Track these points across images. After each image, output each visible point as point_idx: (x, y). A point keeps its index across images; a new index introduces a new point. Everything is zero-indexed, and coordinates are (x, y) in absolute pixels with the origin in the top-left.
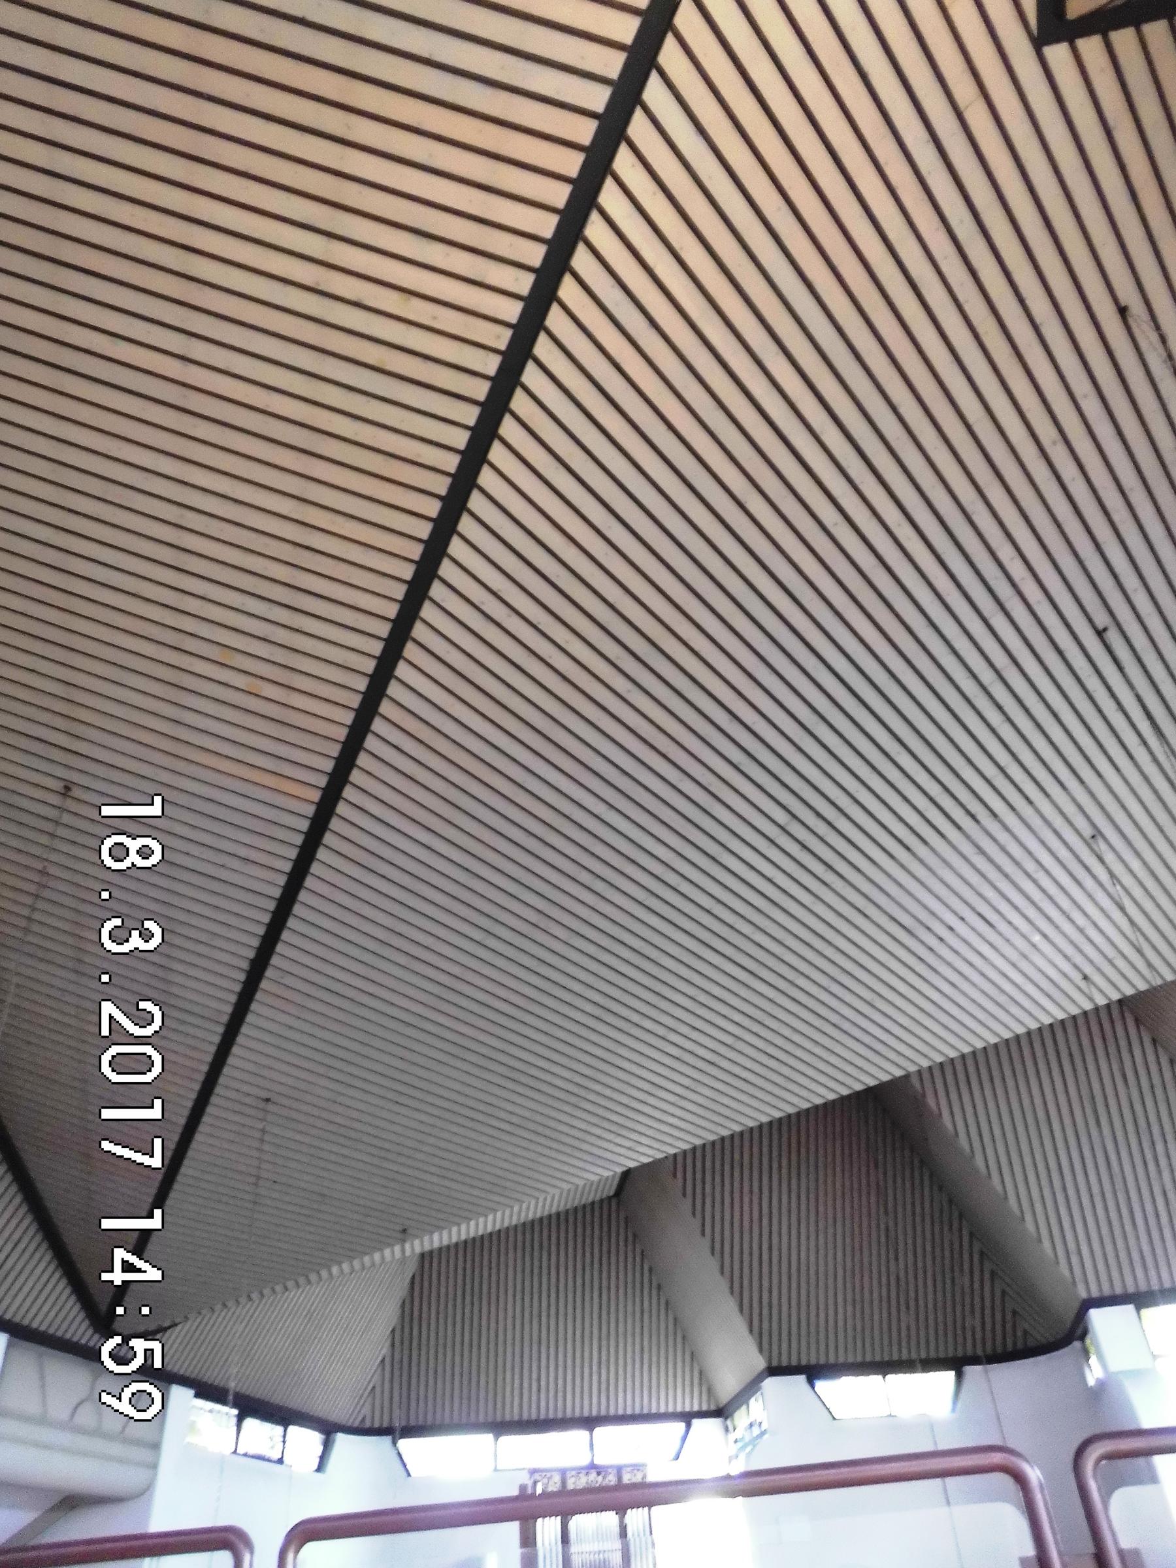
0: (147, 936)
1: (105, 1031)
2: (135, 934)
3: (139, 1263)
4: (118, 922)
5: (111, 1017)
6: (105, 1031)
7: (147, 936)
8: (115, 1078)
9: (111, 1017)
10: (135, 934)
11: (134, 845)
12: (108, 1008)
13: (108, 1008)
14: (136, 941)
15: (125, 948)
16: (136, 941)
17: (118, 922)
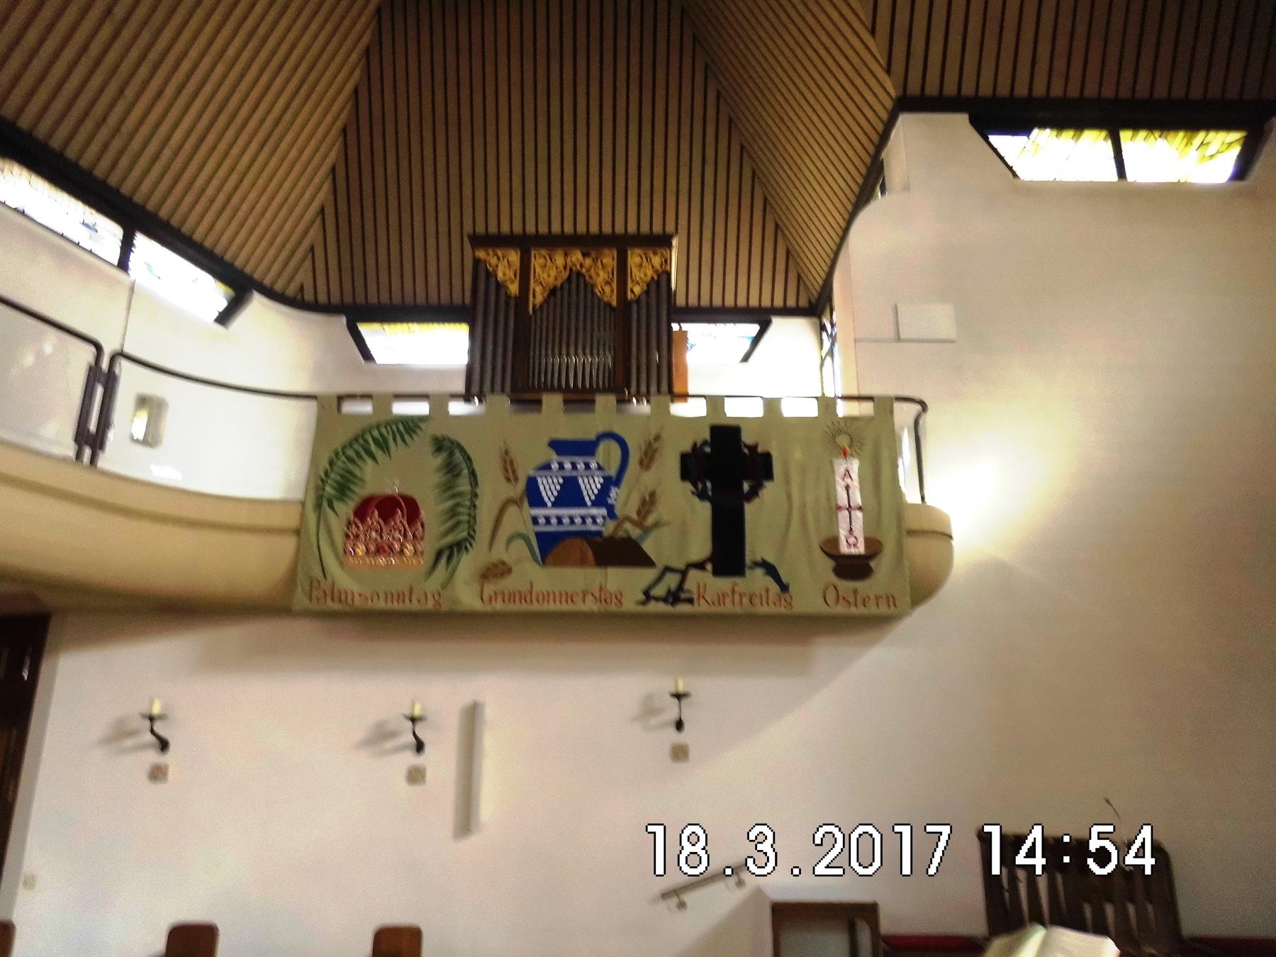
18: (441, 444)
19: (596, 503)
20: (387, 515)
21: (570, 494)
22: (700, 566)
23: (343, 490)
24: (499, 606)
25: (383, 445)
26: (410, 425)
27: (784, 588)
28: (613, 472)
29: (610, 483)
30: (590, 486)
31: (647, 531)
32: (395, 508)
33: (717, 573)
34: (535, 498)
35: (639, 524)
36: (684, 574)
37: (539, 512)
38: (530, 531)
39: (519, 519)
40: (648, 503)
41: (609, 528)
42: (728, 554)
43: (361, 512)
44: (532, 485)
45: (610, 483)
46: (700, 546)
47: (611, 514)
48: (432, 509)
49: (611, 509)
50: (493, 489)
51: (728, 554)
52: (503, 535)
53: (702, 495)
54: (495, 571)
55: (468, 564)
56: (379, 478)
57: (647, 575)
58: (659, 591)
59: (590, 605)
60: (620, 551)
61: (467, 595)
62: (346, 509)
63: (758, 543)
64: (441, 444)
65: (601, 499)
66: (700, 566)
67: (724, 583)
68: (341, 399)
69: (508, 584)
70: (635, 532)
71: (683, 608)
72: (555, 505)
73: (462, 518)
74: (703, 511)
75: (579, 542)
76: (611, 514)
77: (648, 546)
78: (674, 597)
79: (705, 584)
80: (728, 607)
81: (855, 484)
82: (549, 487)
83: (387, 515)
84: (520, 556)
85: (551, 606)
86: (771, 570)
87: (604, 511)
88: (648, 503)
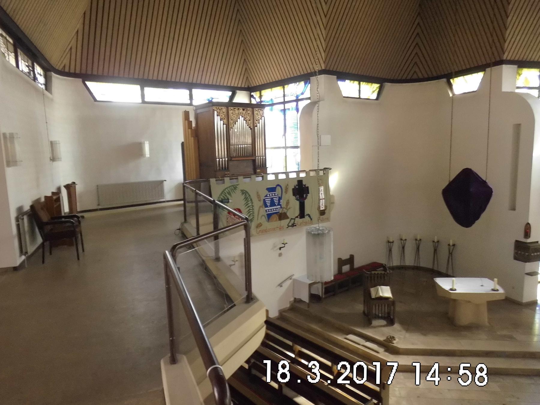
2: (313, 371)
3: (432, 371)
11: (281, 371)
27: (311, 219)
31: (288, 210)
35: (286, 209)
37: (267, 209)
38: (265, 214)
39: (263, 211)
40: (288, 203)
46: (297, 213)
49: (281, 205)
52: (260, 216)
53: (297, 199)
60: (282, 216)
63: (307, 211)
72: (271, 206)
74: (298, 203)
79: (298, 220)
81: (323, 195)
82: (268, 204)
84: (263, 220)
86: (309, 215)
87: (279, 207)
88: (288, 203)
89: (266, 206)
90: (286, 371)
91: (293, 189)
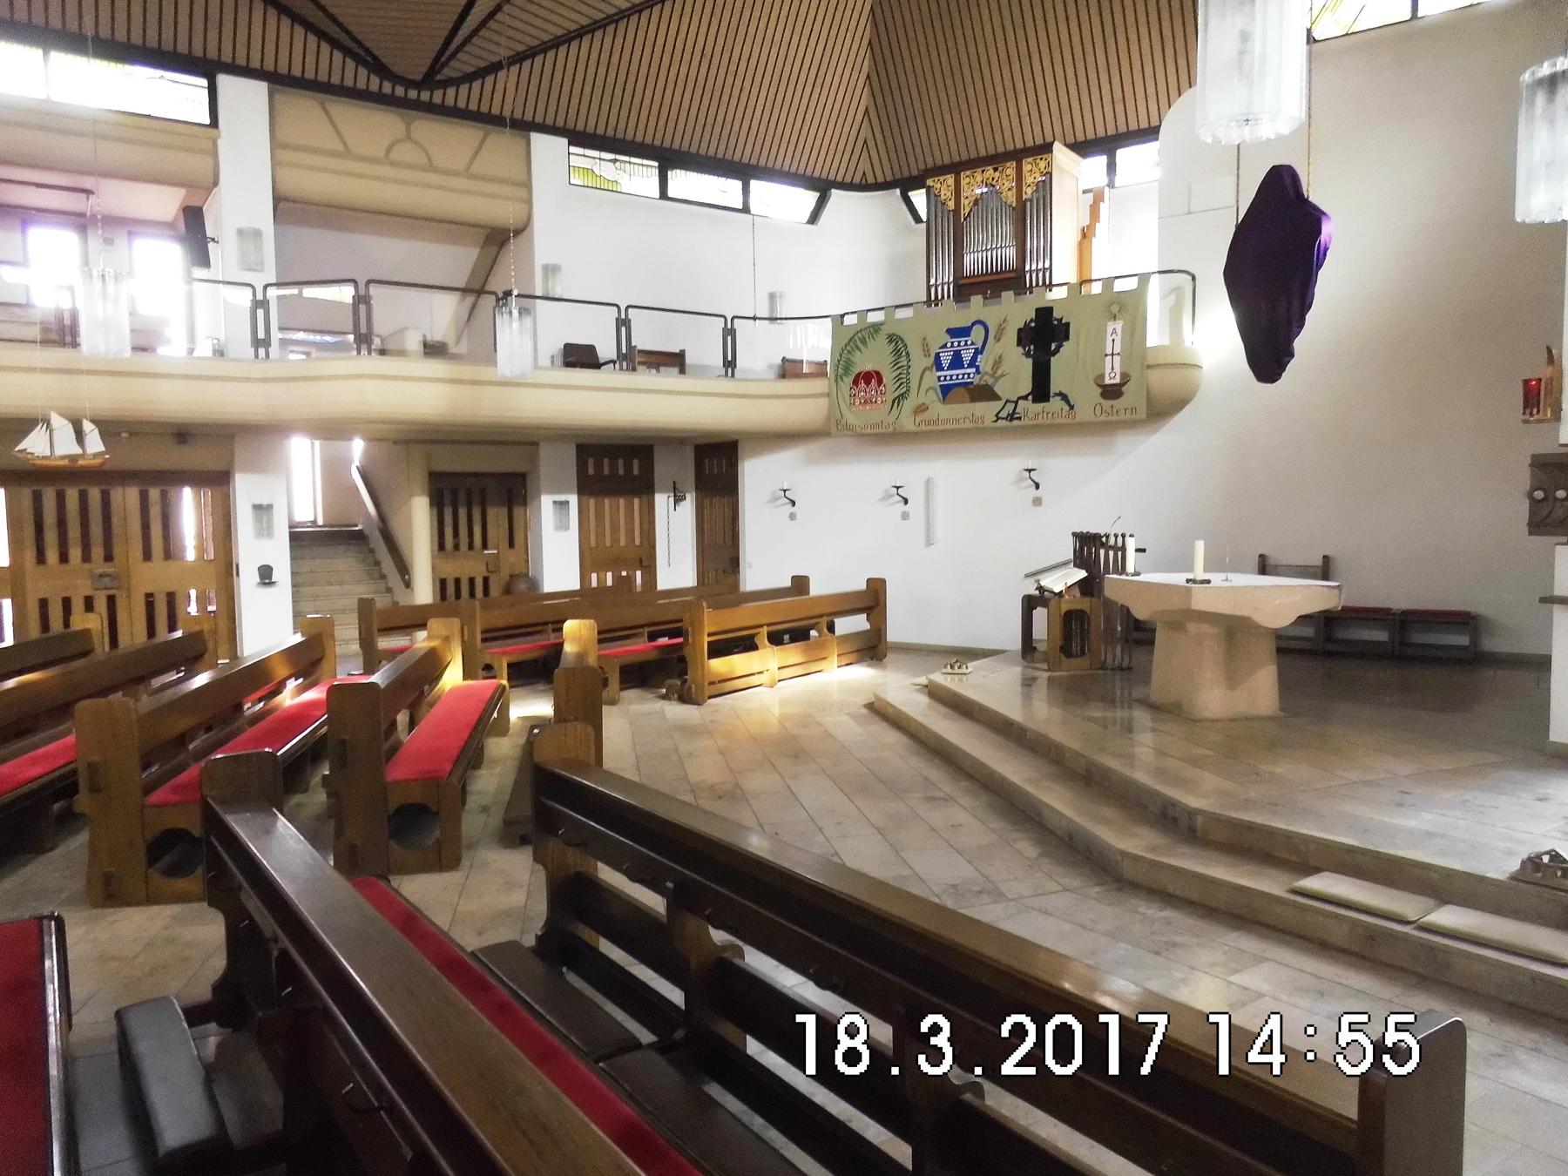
0: (936, 1030)
1: (1031, 1071)
2: (933, 1041)
4: (922, 1059)
5: (1017, 1065)
6: (1031, 1071)
7: (936, 1030)
8: (1078, 1061)
9: (1017, 1065)
10: (933, 1041)
12: (1008, 1068)
13: (1008, 1068)
14: (941, 1041)
15: (948, 1051)
16: (941, 1041)
17: (922, 1059)
18: (893, 338)
19: (970, 366)
20: (868, 383)
21: (957, 362)
22: (1025, 398)
23: (847, 370)
24: (923, 428)
25: (864, 341)
26: (876, 328)
28: (979, 345)
29: (978, 352)
30: (967, 356)
31: (997, 379)
32: (869, 377)
33: (1035, 401)
34: (939, 367)
35: (992, 376)
36: (1016, 403)
41: (976, 380)
42: (1041, 390)
43: (856, 382)
44: (937, 356)
45: (978, 352)
46: (1026, 386)
47: (978, 372)
48: (888, 377)
50: (919, 362)
51: (1041, 390)
54: (921, 409)
55: (908, 405)
56: (864, 363)
57: (997, 405)
58: (1003, 414)
59: (968, 425)
61: (907, 422)
62: (849, 380)
63: (1055, 387)
64: (893, 338)
65: (972, 363)
66: (1025, 398)
67: (1039, 407)
68: (842, 316)
69: (926, 416)
70: (991, 381)
71: (1016, 422)
73: (903, 380)
75: (962, 390)
76: (978, 372)
77: (997, 389)
78: (1011, 417)
80: (1040, 421)
82: (946, 359)
83: (868, 383)
85: (948, 427)
89: (939, 367)
90: (858, 1043)
91: (1020, 330)
